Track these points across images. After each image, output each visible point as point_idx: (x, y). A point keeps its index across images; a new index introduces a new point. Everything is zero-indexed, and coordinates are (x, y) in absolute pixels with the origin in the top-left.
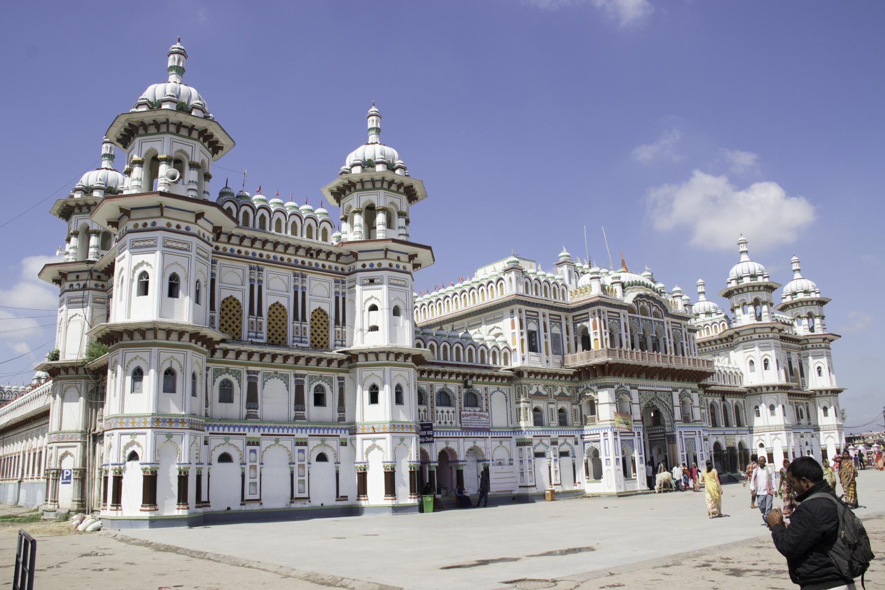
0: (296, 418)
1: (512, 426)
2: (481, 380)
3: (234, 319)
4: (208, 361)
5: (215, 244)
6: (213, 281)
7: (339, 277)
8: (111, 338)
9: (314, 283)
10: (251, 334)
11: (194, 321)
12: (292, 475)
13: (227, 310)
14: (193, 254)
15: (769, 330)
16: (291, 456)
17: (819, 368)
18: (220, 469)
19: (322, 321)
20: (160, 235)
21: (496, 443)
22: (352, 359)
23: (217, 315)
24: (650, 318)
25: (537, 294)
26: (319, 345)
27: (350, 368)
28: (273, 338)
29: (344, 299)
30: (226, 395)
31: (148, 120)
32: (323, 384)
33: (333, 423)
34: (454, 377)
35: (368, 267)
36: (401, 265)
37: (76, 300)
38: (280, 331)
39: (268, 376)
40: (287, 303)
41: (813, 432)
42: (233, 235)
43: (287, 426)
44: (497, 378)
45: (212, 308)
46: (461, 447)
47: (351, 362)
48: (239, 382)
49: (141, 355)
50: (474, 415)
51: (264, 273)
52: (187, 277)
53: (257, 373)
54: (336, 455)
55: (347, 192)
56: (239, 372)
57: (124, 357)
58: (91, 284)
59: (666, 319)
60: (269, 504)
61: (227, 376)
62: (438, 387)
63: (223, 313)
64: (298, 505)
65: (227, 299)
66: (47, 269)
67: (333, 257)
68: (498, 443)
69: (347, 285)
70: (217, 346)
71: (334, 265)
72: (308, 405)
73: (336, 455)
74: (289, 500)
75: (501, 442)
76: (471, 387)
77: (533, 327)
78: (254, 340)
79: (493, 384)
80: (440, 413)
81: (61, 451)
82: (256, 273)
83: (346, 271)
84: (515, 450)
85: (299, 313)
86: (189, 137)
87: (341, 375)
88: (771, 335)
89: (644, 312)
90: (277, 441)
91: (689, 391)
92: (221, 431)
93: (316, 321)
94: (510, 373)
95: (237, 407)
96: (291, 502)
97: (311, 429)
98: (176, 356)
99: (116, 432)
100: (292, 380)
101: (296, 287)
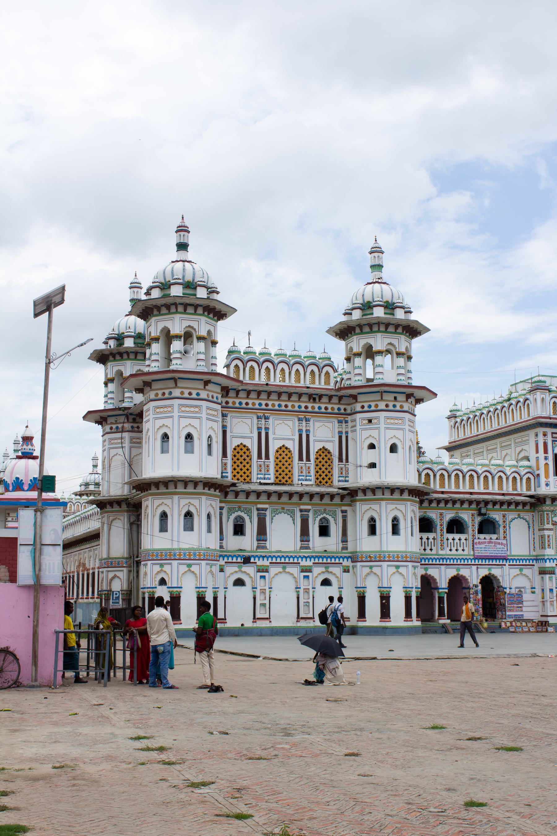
0: (302, 548)
1: (534, 553)
2: (498, 507)
3: (245, 463)
4: (221, 502)
5: (224, 400)
6: (224, 433)
7: (341, 418)
8: (145, 486)
9: (317, 424)
10: (259, 476)
12: (298, 598)
13: (238, 456)
14: (204, 416)
16: (296, 581)
18: (235, 592)
19: (326, 459)
20: (176, 402)
21: (516, 571)
22: (351, 495)
23: (229, 461)
26: (324, 482)
27: (352, 501)
28: (280, 477)
29: (347, 437)
30: (239, 530)
31: (159, 303)
32: (328, 516)
33: (336, 553)
34: (466, 505)
35: (366, 409)
36: (398, 405)
37: (116, 441)
38: (287, 471)
39: (275, 512)
40: (294, 447)
42: (239, 391)
43: (293, 555)
44: (517, 504)
45: (225, 454)
46: (474, 576)
47: (353, 497)
48: (250, 518)
49: (165, 501)
50: (489, 542)
51: (271, 421)
52: (200, 435)
53: (265, 509)
54: (339, 580)
55: (349, 335)
56: (250, 510)
57: (153, 504)
58: (127, 426)
60: (275, 623)
61: (239, 513)
62: (449, 516)
63: (235, 459)
64: (303, 624)
65: (238, 446)
66: (90, 415)
67: (335, 400)
69: (350, 424)
70: (228, 490)
71: (336, 407)
72: (313, 537)
73: (339, 580)
74: (296, 620)
75: (521, 570)
76: (485, 514)
78: (262, 481)
79: (512, 511)
80: (450, 541)
81: (111, 575)
82: (263, 420)
83: (349, 411)
84: (538, 578)
85: (304, 453)
86: (195, 313)
87: (344, 508)
90: (284, 568)
92: (234, 560)
93: (320, 459)
96: (297, 621)
97: (314, 558)
98: (192, 501)
99: (149, 563)
100: (298, 515)
101: (300, 431)
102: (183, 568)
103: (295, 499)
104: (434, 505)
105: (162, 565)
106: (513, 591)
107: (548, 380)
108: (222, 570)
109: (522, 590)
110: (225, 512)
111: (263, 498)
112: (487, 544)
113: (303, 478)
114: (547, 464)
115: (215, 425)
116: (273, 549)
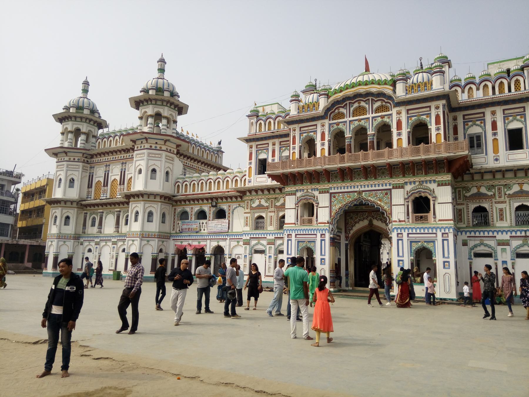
5: (92, 160)
11: (64, 195)
24: (367, 116)
25: (269, 129)
39: (108, 214)
44: (236, 197)
51: (110, 167)
53: (103, 213)
59: (394, 111)
62: (196, 208)
68: (236, 243)
75: (238, 242)
77: (262, 156)
89: (361, 111)
91: (433, 186)
94: (239, 194)
101: (122, 169)
105: (52, 242)
107: (260, 109)
108: (82, 244)
109: (240, 256)
110: (88, 215)
112: (220, 225)
114: (250, 167)
115: (76, 173)
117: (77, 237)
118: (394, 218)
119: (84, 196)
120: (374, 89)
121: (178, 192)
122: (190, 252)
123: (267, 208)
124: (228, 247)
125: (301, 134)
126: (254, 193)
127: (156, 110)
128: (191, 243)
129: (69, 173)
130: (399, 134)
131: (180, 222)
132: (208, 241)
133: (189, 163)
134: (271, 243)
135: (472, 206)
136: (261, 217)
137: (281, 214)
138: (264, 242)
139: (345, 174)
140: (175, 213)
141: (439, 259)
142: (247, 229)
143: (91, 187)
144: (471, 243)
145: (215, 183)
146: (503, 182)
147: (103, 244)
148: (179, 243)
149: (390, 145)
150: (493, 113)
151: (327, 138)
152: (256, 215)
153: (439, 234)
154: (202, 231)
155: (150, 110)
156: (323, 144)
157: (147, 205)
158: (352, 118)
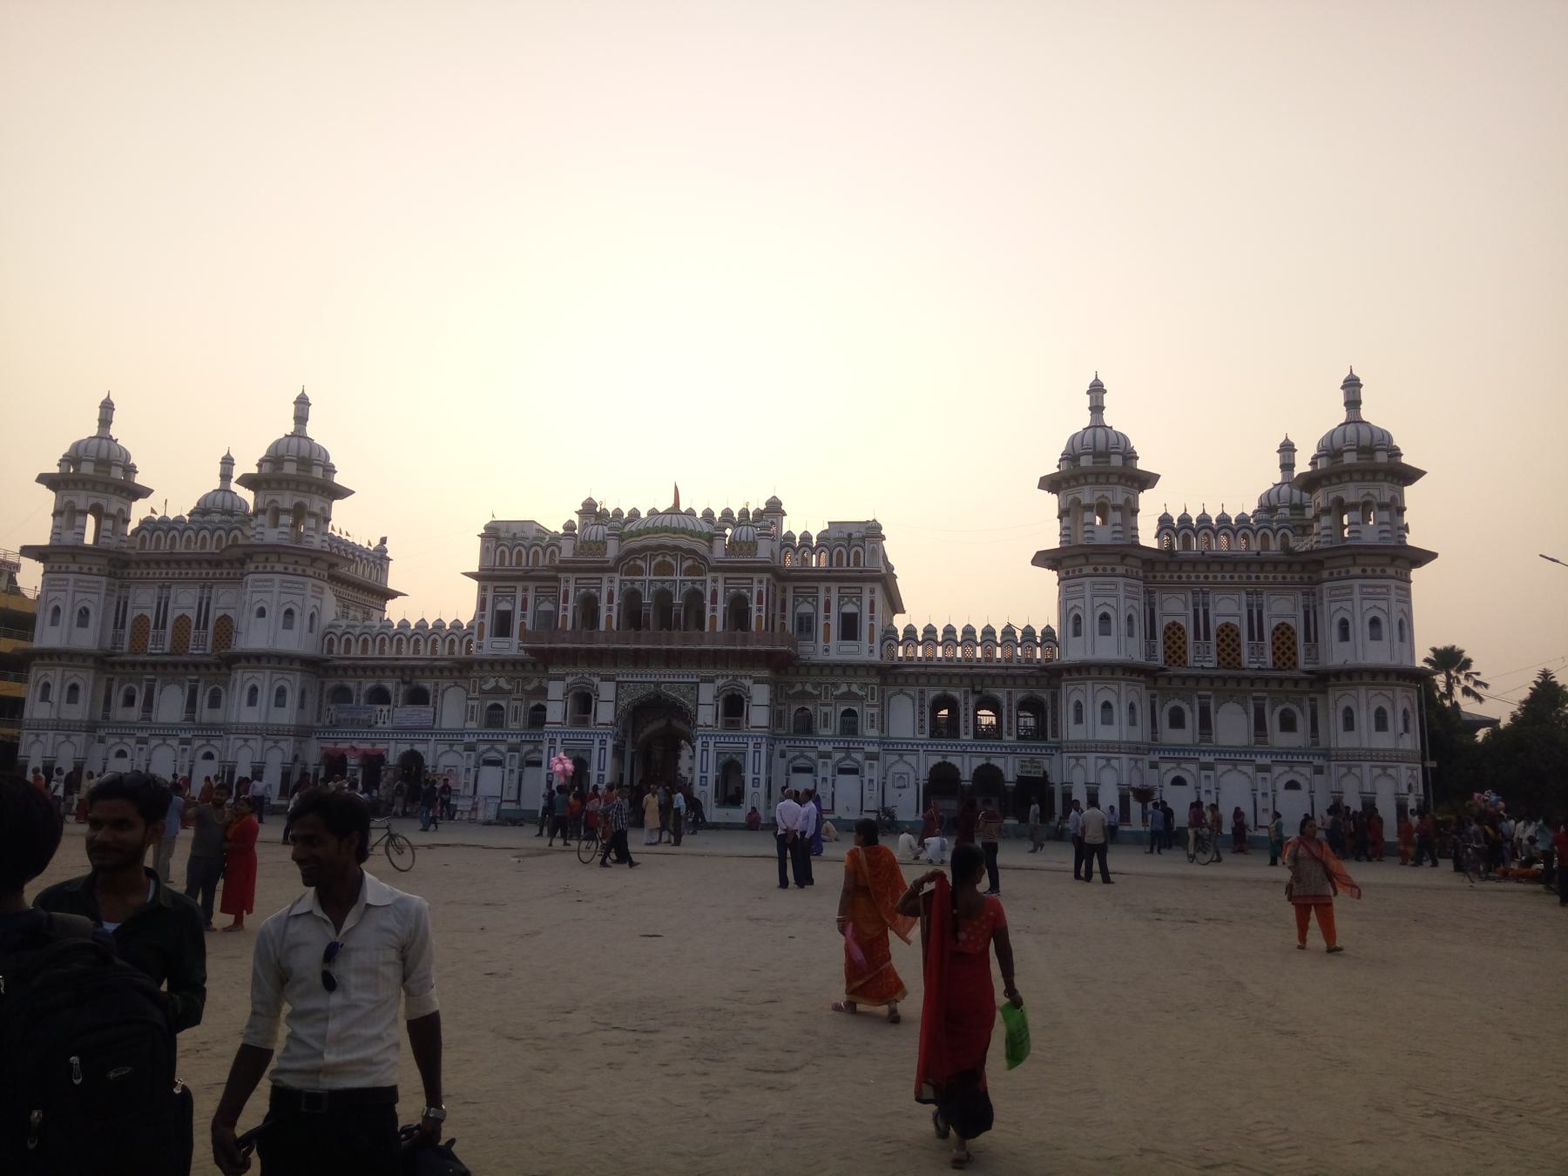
15: (1083, 560)
17: (1344, 625)
25: (519, 564)
30: (129, 701)
34: (388, 673)
36: (269, 566)
39: (165, 683)
40: (192, 615)
41: (1317, 762)
44: (451, 670)
59: (709, 577)
88: (1088, 570)
91: (748, 682)
95: (135, 713)
100: (187, 684)
101: (201, 599)
102: (32, 738)
103: (181, 670)
104: (350, 673)
106: (440, 770)
108: (102, 740)
111: (149, 669)
113: (201, 646)
115: (94, 598)
116: (160, 720)
117: (91, 727)
118: (700, 722)
119: (108, 644)
120: (685, 542)
121: (330, 651)
122: (353, 761)
123: (510, 692)
124: (430, 754)
125: (577, 589)
126: (487, 667)
127: (297, 500)
128: (354, 745)
129: (79, 596)
130: (714, 610)
131: (332, 707)
132: (392, 743)
133: (343, 590)
134: (513, 749)
135: (795, 708)
136: (497, 707)
137: (533, 703)
138: (503, 748)
139: (639, 658)
140: (322, 689)
141: (749, 776)
142: (472, 725)
143: (123, 627)
144: (790, 755)
145: (408, 640)
146: (831, 680)
147: (154, 742)
148: (330, 745)
149: (701, 625)
150: (828, 590)
151: (616, 600)
152: (489, 703)
153: (751, 745)
154: (380, 724)
155: (287, 500)
156: (610, 609)
157: (276, 676)
158: (652, 577)
